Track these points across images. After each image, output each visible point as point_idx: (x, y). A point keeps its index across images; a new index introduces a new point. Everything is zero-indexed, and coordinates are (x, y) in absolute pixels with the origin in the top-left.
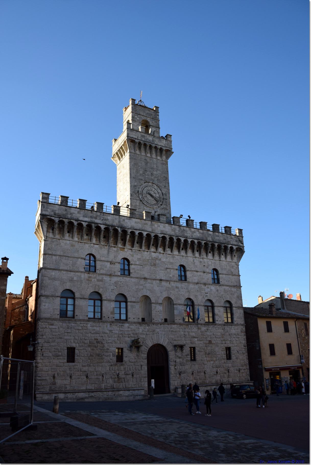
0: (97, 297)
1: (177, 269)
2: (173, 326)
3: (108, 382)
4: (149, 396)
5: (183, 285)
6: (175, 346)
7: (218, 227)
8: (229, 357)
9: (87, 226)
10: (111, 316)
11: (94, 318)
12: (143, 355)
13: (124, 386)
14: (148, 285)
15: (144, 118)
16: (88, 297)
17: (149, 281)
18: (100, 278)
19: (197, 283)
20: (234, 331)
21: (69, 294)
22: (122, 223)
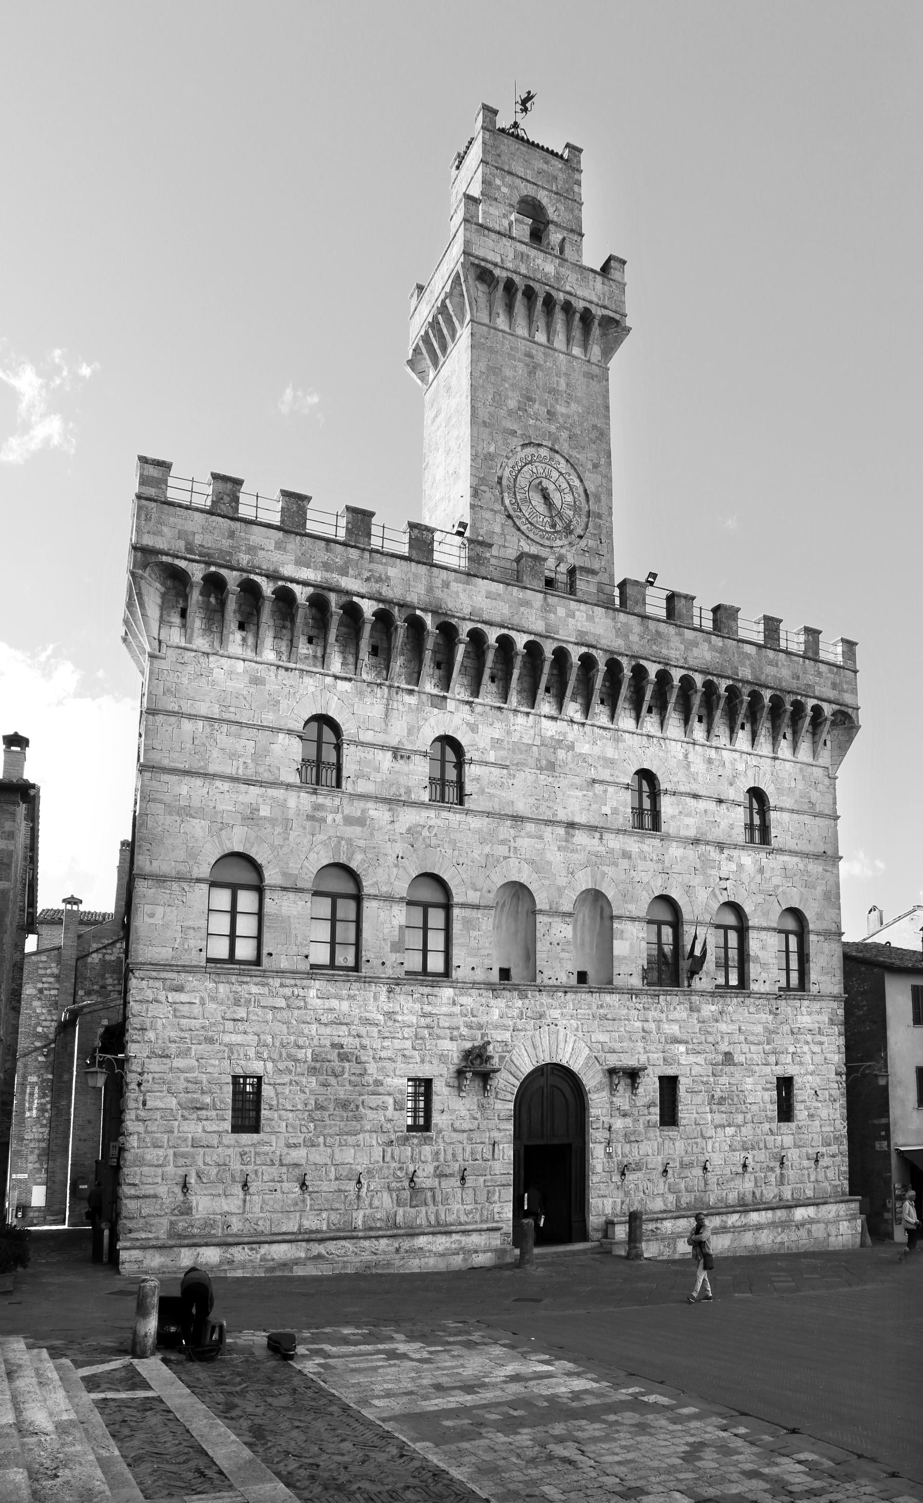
0: (343, 887)
2: (608, 998)
3: (376, 1203)
4: (517, 1251)
5: (645, 848)
6: (612, 1072)
8: (785, 1112)
10: (393, 958)
11: (332, 966)
12: (499, 1105)
13: (432, 1219)
14: (524, 843)
15: (527, 190)
16: (309, 885)
17: (530, 827)
18: (355, 809)
19: (696, 842)
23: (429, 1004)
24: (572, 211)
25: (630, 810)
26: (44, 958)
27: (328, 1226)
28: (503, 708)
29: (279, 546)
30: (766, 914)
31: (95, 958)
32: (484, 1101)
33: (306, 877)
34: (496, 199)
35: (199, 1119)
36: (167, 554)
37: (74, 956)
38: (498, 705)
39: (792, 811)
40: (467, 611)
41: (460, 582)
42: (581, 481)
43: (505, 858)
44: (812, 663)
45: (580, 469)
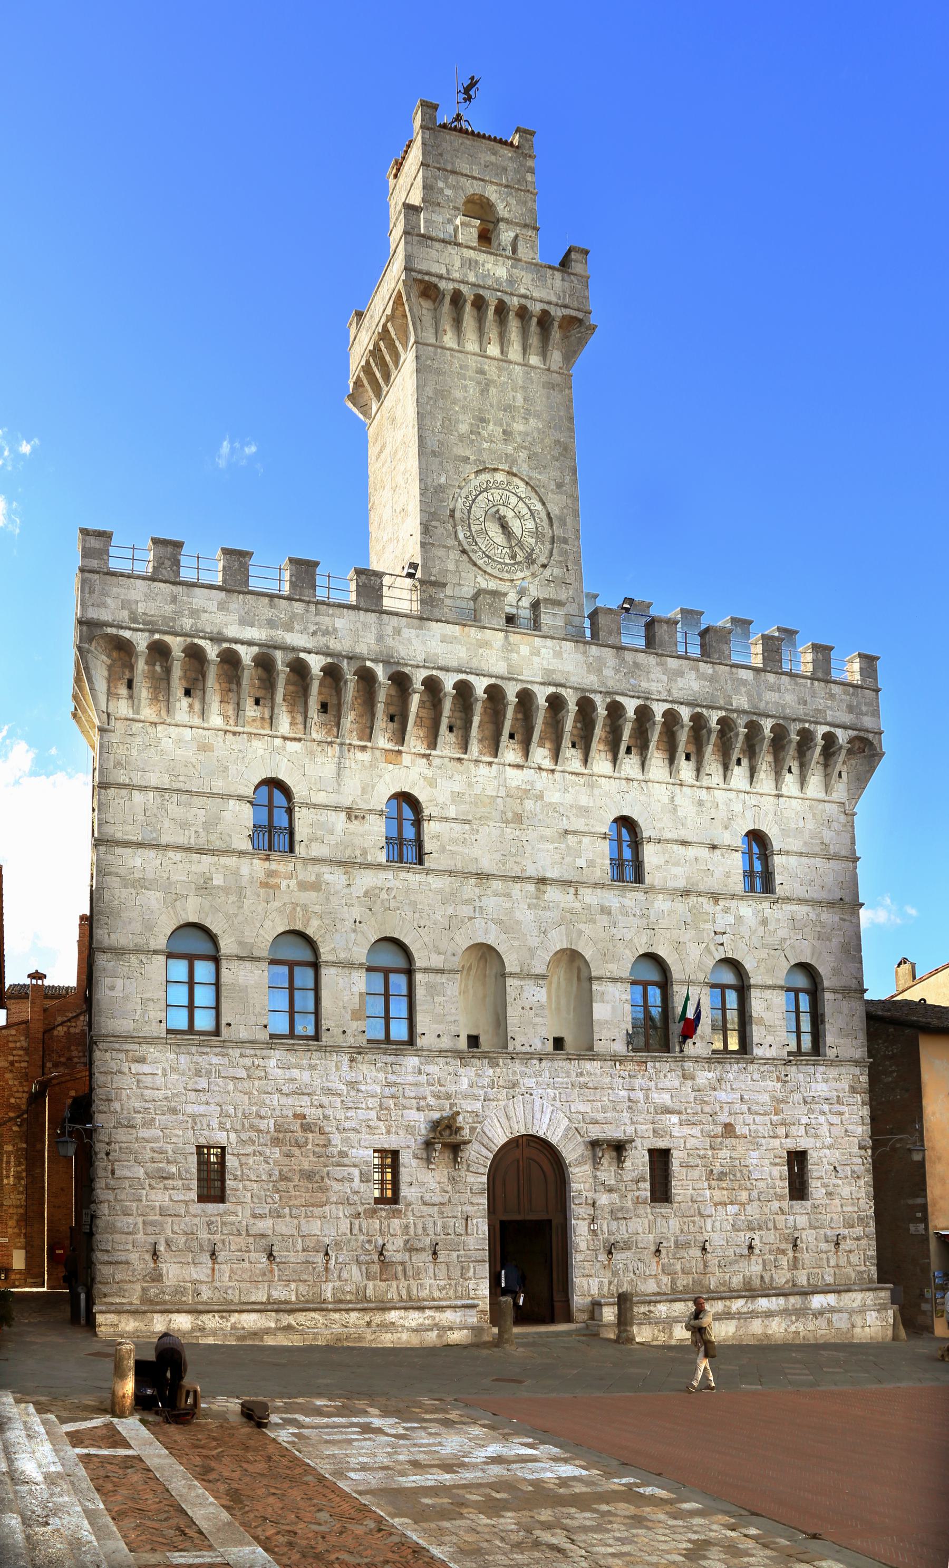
2: (588, 1066)
3: (345, 1275)
6: (594, 1144)
8: (798, 1188)
11: (292, 1035)
12: (471, 1178)
13: (404, 1293)
14: (491, 903)
16: (265, 954)
17: (496, 885)
18: (309, 874)
19: (686, 893)
23: (393, 1073)
25: (609, 862)
26: (13, 1032)
27: (297, 1297)
28: (463, 759)
29: (222, 607)
30: (771, 971)
31: (61, 1031)
32: (455, 1174)
33: (262, 946)
35: (166, 1188)
36: (112, 626)
37: (41, 1030)
38: (458, 756)
39: (801, 854)
40: (420, 658)
41: (412, 628)
42: (544, 504)
43: (470, 919)
44: (822, 684)
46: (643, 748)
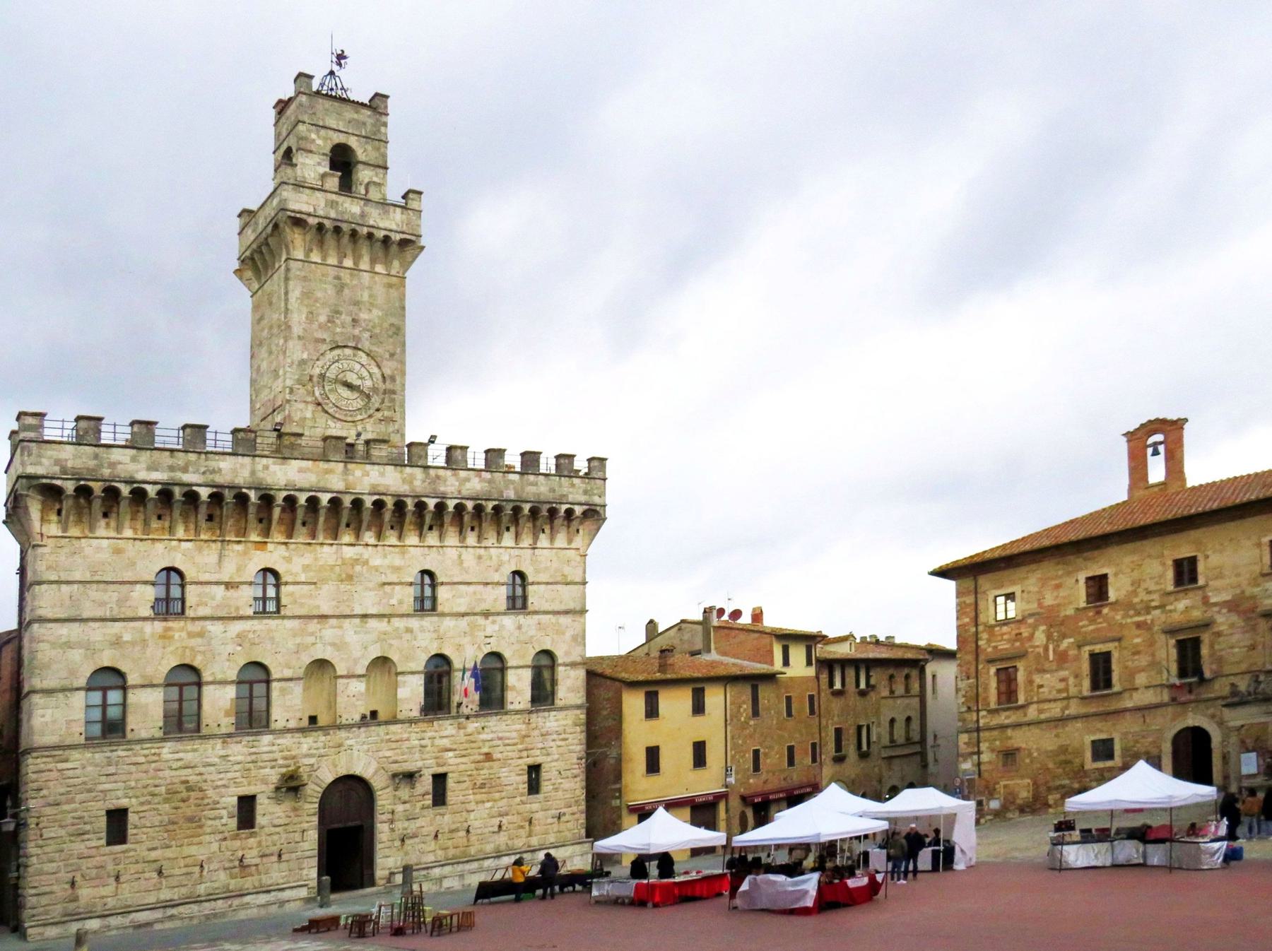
0: (187, 678)
1: (411, 584)
6: (394, 776)
7: (538, 461)
8: (534, 786)
9: (159, 493)
12: (307, 806)
15: (340, 138)
17: (333, 622)
18: (198, 626)
20: (555, 724)
21: (110, 678)
22: (260, 475)
24: (378, 149)
32: (297, 805)
34: (311, 152)
39: (548, 583)
42: (379, 367)
45: (379, 359)
46: (442, 525)
